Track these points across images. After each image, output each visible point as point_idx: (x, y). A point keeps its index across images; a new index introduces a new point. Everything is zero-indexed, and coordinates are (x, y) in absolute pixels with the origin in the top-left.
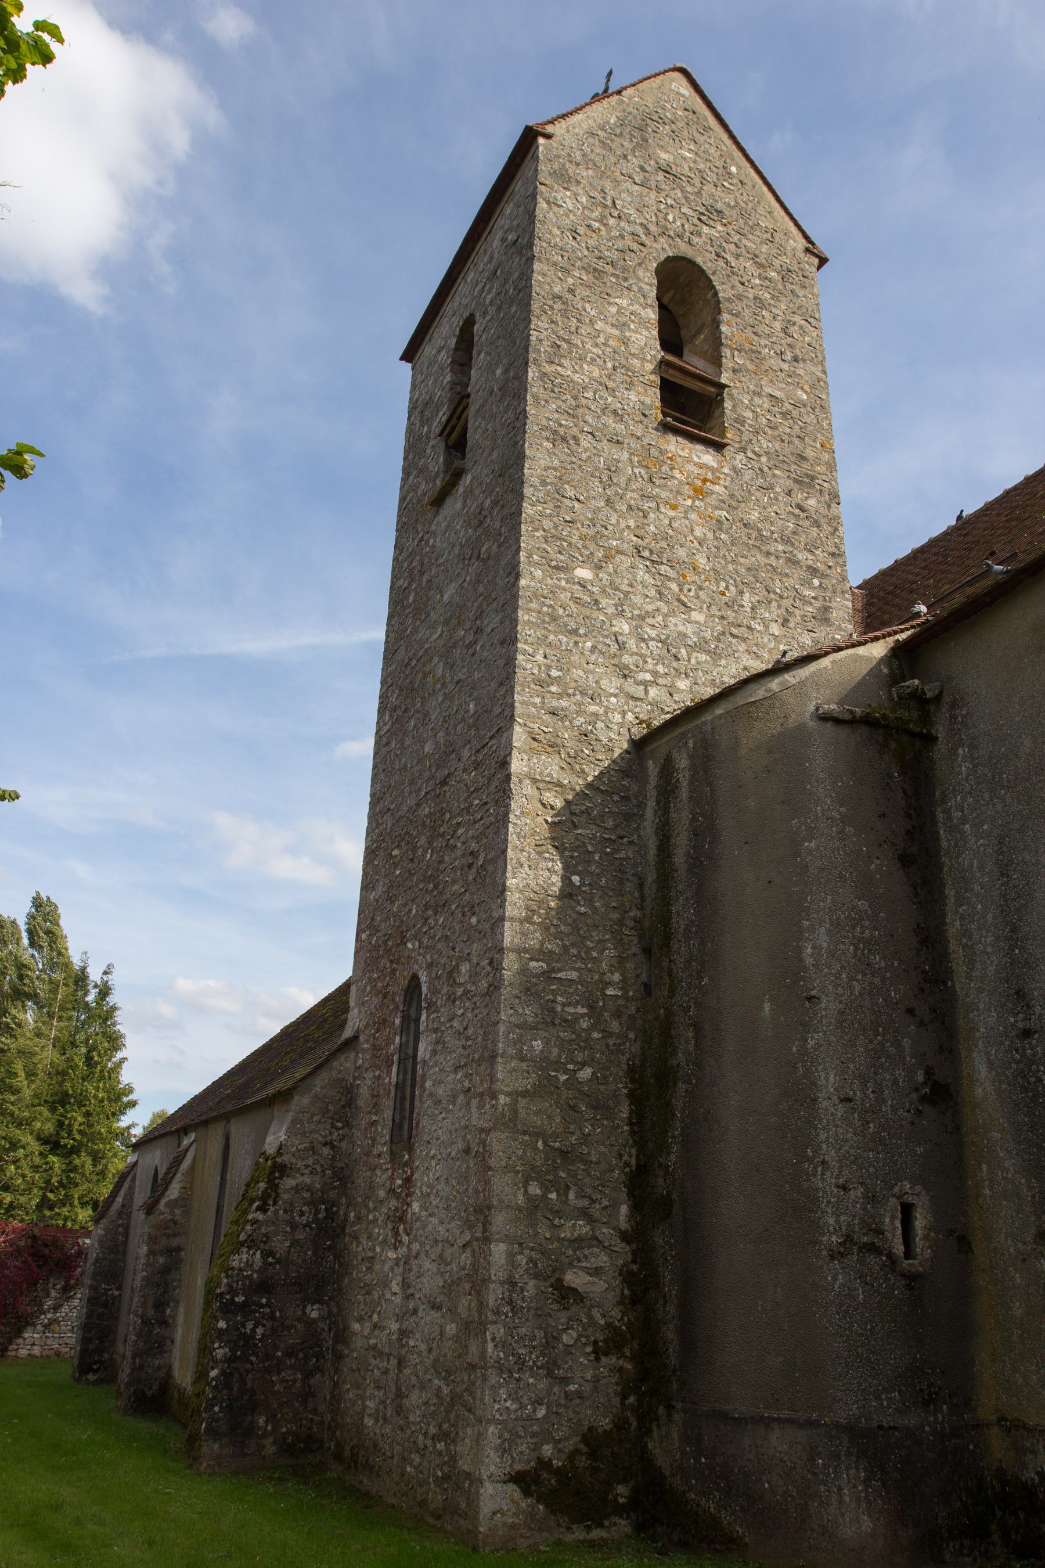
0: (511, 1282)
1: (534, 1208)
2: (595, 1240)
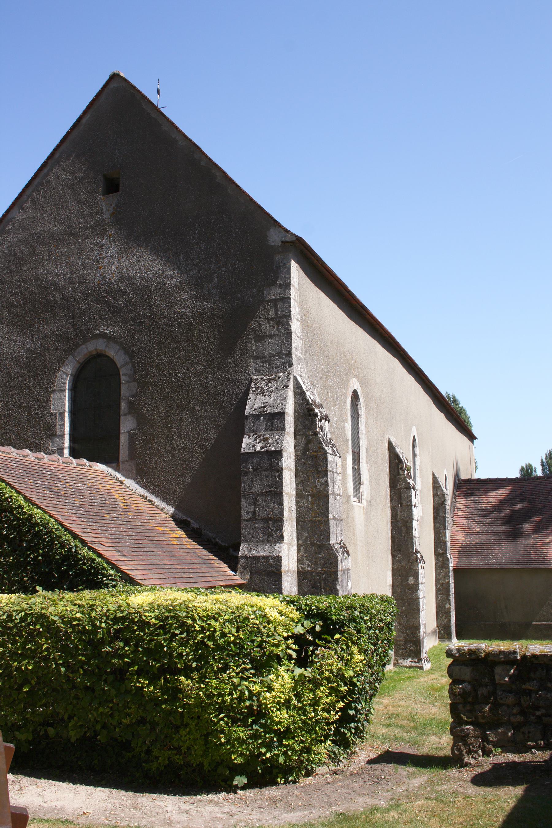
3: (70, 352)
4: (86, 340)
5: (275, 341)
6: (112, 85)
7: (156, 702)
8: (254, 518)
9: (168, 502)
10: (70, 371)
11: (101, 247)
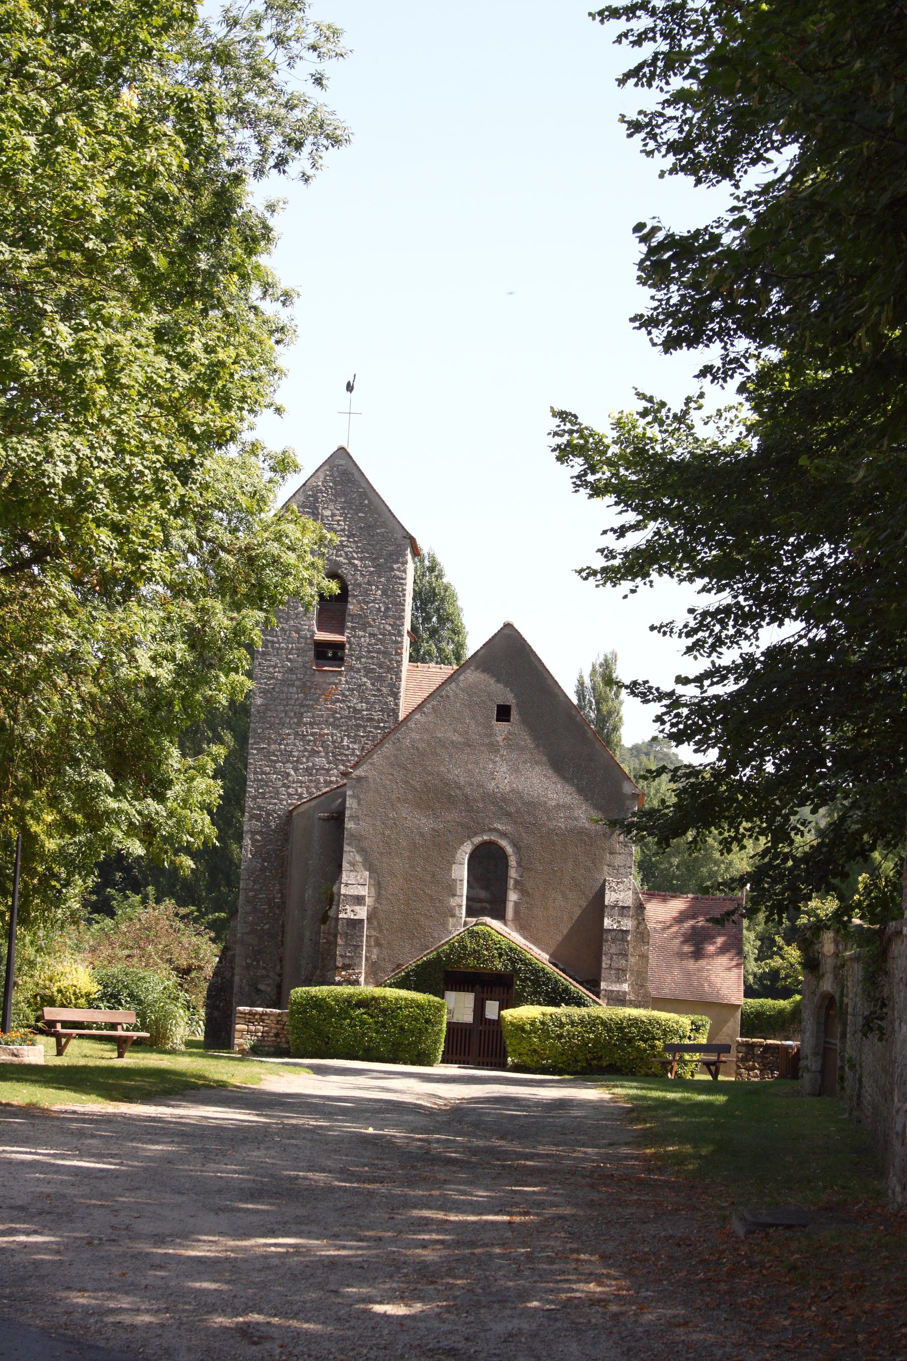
0: (241, 987)
1: (248, 967)
2: (268, 976)
3: (469, 838)
4: (483, 831)
5: (622, 857)
6: (506, 631)
7: (645, 1050)
8: (610, 968)
9: (543, 950)
10: (469, 851)
11: (495, 762)
